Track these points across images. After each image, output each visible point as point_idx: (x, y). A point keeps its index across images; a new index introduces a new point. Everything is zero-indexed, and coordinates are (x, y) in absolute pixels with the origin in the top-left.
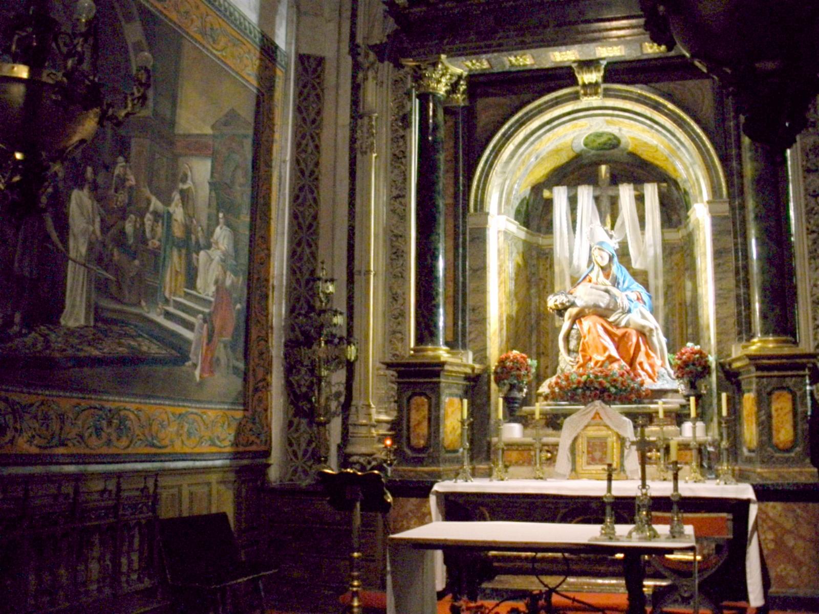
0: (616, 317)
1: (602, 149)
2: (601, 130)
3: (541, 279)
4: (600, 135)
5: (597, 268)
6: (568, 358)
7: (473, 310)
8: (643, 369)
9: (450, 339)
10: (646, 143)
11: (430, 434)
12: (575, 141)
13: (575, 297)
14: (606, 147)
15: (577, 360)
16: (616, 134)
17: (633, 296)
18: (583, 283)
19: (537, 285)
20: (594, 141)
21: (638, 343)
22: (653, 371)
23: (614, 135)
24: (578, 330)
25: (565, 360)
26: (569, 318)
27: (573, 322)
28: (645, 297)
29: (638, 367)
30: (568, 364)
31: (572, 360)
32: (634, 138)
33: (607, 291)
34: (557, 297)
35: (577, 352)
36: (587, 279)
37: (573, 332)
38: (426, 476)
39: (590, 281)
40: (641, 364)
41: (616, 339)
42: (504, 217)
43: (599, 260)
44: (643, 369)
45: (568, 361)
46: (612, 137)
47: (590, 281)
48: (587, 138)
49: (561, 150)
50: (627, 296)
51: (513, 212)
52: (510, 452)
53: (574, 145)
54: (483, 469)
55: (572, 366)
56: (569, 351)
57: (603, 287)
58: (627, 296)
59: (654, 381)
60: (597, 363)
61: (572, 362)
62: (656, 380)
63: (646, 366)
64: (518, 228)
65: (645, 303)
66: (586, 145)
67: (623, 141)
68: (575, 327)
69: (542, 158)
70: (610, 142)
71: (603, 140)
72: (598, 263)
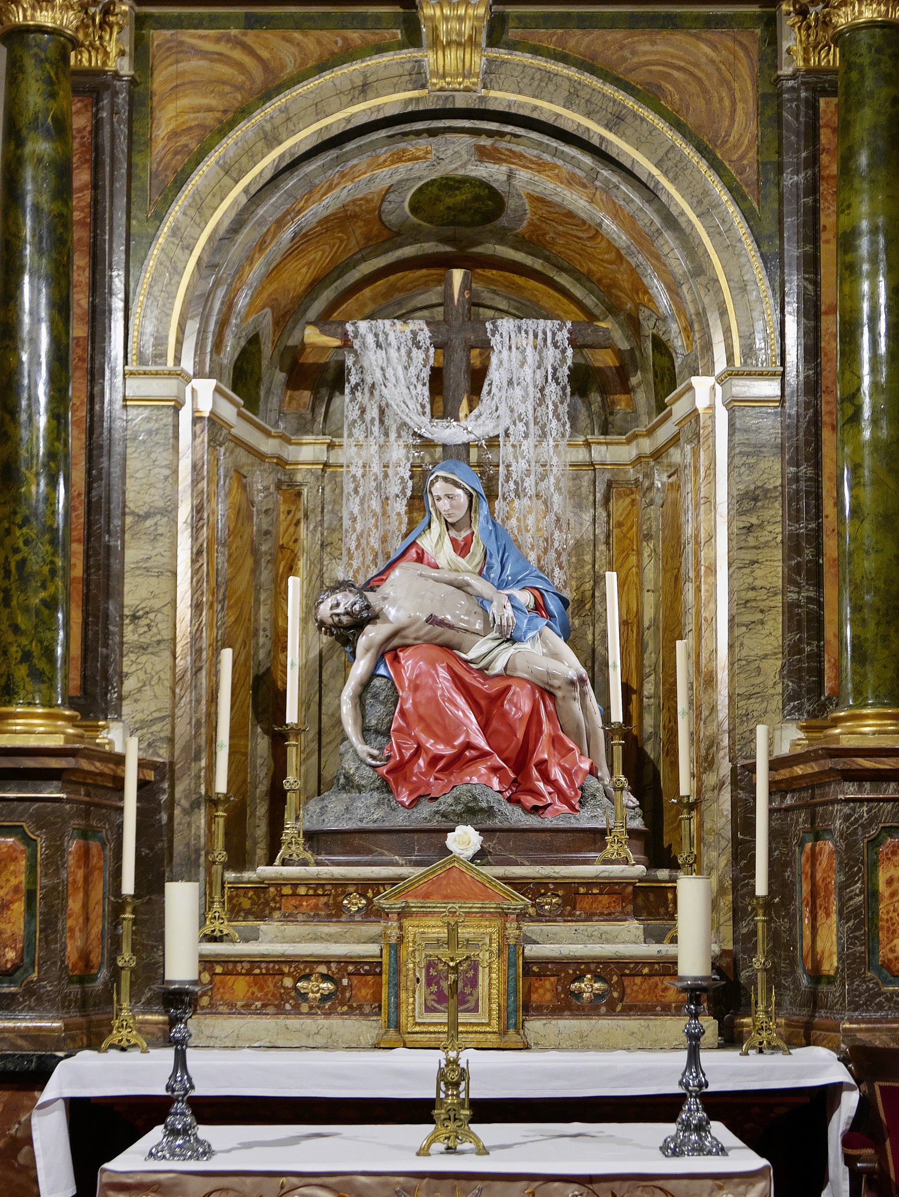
0: (484, 649)
1: (452, 223)
2: (461, 172)
3: (282, 547)
4: (450, 184)
5: (436, 526)
6: (362, 749)
7: (135, 618)
8: (546, 778)
9: (74, 692)
10: (570, 214)
11: (29, 936)
12: (391, 197)
13: (384, 599)
14: (464, 217)
15: (386, 753)
16: (495, 185)
17: (525, 598)
18: (403, 564)
19: (274, 561)
20: (438, 199)
21: (535, 711)
22: (571, 785)
23: (490, 188)
24: (389, 678)
25: (355, 751)
26: (367, 650)
27: (379, 659)
28: (553, 605)
29: (535, 773)
30: (362, 761)
31: (375, 752)
32: (539, 200)
33: (461, 587)
34: (339, 596)
35: (386, 734)
36: (413, 553)
37: (377, 682)
38: (20, 1042)
39: (420, 558)
40: (543, 766)
41: (483, 703)
42: (213, 383)
43: (444, 505)
44: (546, 778)
45: (363, 755)
46: (485, 192)
47: (420, 558)
48: (420, 190)
49: (355, 216)
50: (510, 598)
51: (228, 374)
52: (230, 979)
53: (386, 207)
54: (157, 1023)
55: (374, 767)
56: (365, 731)
57: (452, 576)
58: (510, 598)
59: (572, 807)
60: (435, 759)
61: (373, 757)
62: (577, 807)
63: (556, 773)
64: (240, 415)
65: (550, 616)
66: (414, 209)
67: (511, 203)
68: (382, 671)
69: (305, 235)
70: (476, 205)
71: (460, 197)
72: (439, 514)
